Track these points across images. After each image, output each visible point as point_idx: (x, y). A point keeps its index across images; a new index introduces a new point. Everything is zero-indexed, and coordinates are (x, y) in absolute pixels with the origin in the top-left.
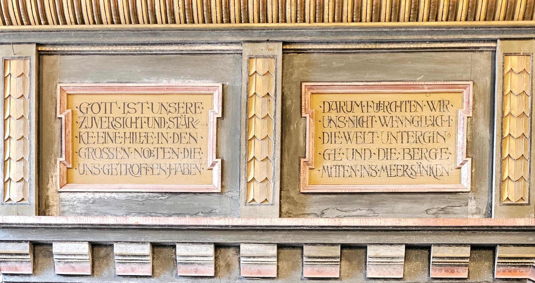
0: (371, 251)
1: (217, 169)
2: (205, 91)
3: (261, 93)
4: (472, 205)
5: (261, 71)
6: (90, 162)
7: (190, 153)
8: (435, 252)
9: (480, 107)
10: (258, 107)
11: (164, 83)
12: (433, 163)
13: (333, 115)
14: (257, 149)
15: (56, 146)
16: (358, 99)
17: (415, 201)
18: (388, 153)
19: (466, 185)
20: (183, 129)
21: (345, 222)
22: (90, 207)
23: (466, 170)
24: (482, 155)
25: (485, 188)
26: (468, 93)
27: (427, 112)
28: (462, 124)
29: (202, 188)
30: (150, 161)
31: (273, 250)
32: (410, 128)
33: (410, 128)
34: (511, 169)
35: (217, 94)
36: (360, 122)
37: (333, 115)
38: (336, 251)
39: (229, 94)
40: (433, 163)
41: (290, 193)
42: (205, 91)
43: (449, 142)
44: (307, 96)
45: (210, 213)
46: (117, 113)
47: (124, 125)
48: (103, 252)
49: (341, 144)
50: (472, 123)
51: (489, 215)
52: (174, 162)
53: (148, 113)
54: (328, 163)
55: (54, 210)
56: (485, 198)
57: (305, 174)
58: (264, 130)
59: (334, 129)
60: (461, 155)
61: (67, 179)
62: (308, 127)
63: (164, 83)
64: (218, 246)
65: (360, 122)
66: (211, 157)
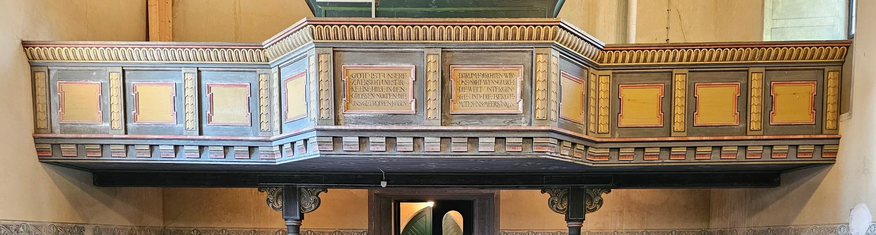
0: (481, 140)
1: (413, 104)
2: (409, 69)
3: (432, 70)
4: (523, 119)
5: (433, 62)
6: (357, 100)
7: (401, 96)
8: (508, 140)
9: (526, 76)
10: (431, 77)
11: (389, 65)
12: (507, 101)
13: (464, 79)
14: (431, 95)
15: (342, 93)
16: (474, 72)
17: (499, 118)
18: (488, 96)
19: (521, 110)
20: (398, 85)
21: (470, 128)
23: (521, 104)
24: (528, 97)
25: (529, 112)
26: (521, 70)
27: (504, 78)
28: (519, 84)
29: (407, 112)
30: (384, 99)
31: (439, 140)
32: (497, 85)
33: (497, 85)
34: (539, 104)
35: (413, 70)
36: (475, 82)
37: (464, 79)
38: (466, 140)
39: (418, 70)
40: (507, 101)
41: (446, 115)
42: (409, 69)
43: (514, 91)
44: (452, 71)
45: (410, 123)
46: (369, 78)
47: (372, 83)
48: (364, 140)
49: (467, 92)
50: (523, 84)
51: (530, 124)
52: (394, 100)
53: (382, 78)
54: (461, 101)
55: (342, 122)
56: (529, 117)
57: (452, 106)
58: (434, 86)
59: (464, 85)
60: (518, 98)
61: (347, 108)
62: (453, 84)
63: (389, 65)
64: (414, 138)
65: (475, 82)
66: (410, 98)
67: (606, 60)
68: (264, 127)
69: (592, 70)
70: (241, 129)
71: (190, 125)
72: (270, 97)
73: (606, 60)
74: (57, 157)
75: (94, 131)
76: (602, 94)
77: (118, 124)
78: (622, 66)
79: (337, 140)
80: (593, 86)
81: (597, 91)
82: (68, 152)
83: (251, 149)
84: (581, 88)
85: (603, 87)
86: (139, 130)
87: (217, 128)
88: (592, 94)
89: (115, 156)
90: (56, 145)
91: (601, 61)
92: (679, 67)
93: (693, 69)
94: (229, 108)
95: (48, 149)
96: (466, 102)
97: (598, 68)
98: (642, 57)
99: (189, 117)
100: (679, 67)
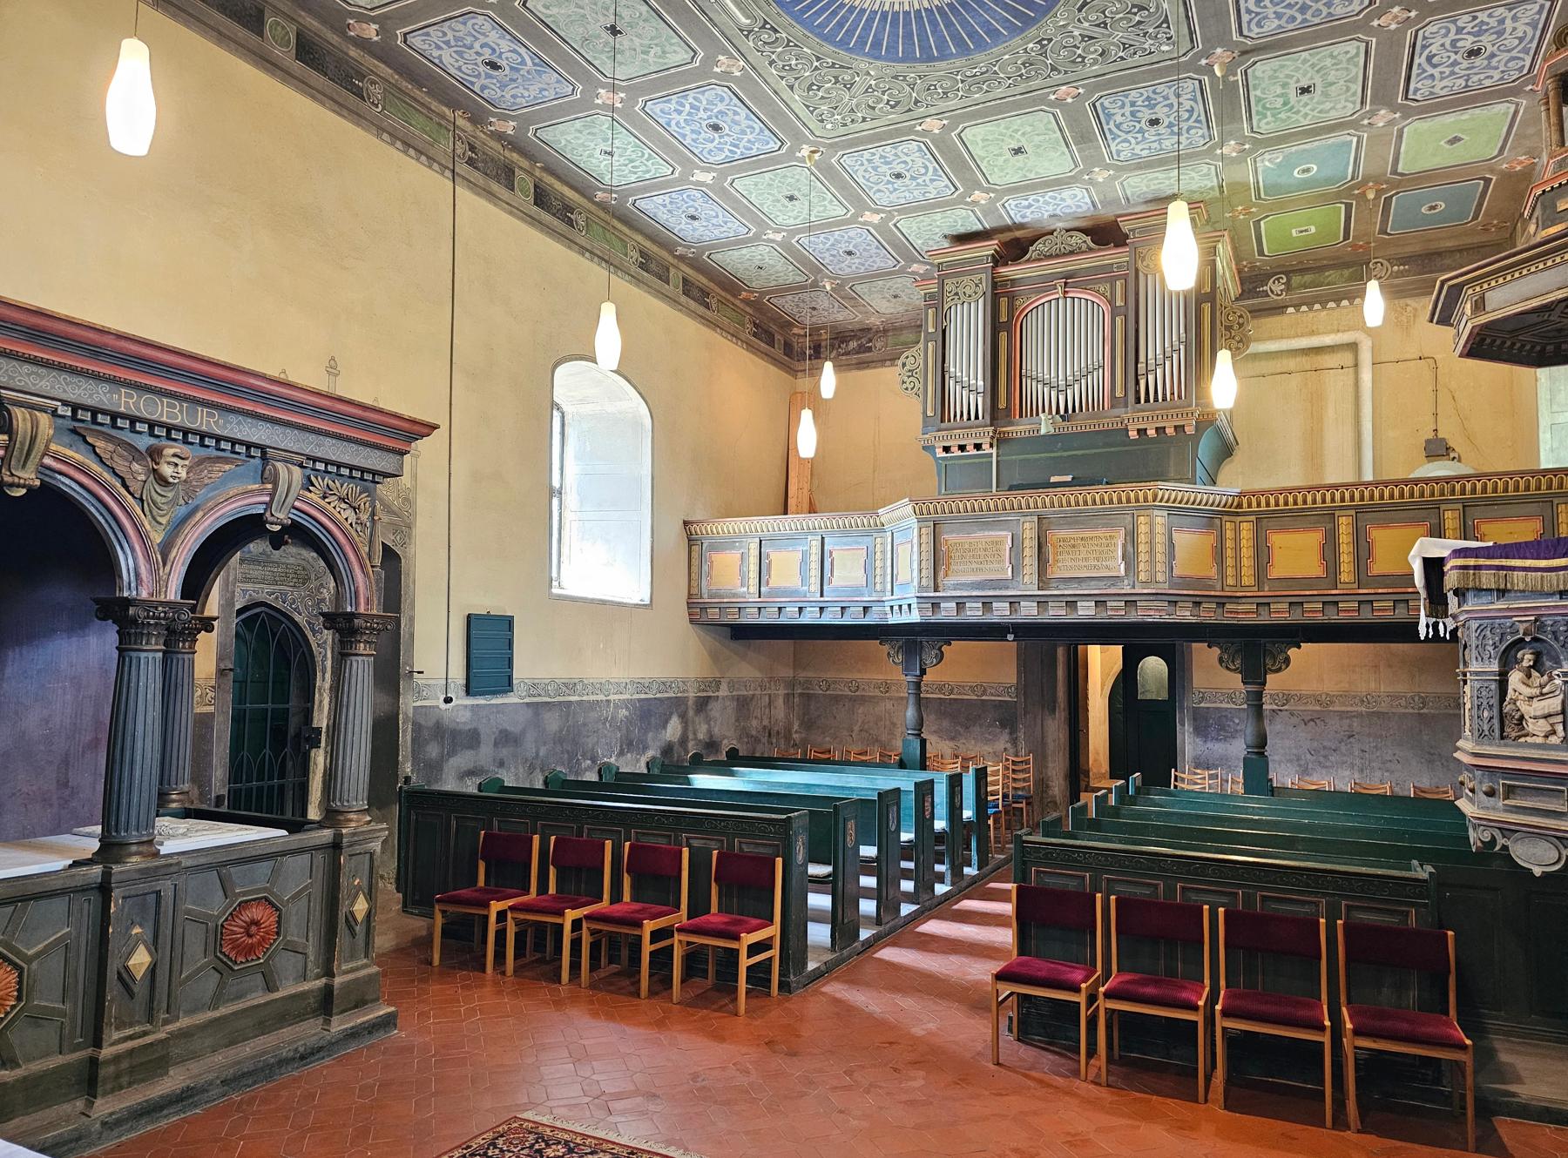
22: (956, 587)
67: (1245, 505)
68: (878, 587)
69: (1226, 518)
70: (857, 590)
71: (813, 588)
72: (884, 560)
73: (1245, 505)
74: (704, 619)
75: (735, 595)
76: (1244, 542)
77: (754, 589)
78: (1274, 513)
79: (935, 606)
80: (1229, 534)
81: (1237, 540)
82: (713, 614)
83: (866, 609)
84: (1211, 539)
85: (1244, 533)
86: (770, 595)
87: (836, 590)
88: (1229, 544)
89: (750, 617)
90: (704, 608)
91: (1240, 505)
92: (1341, 508)
93: (1360, 510)
94: (848, 572)
95: (697, 611)
96: (1062, 567)
97: (1237, 514)
98: (1291, 499)
99: (813, 580)
100: (1341, 508)
